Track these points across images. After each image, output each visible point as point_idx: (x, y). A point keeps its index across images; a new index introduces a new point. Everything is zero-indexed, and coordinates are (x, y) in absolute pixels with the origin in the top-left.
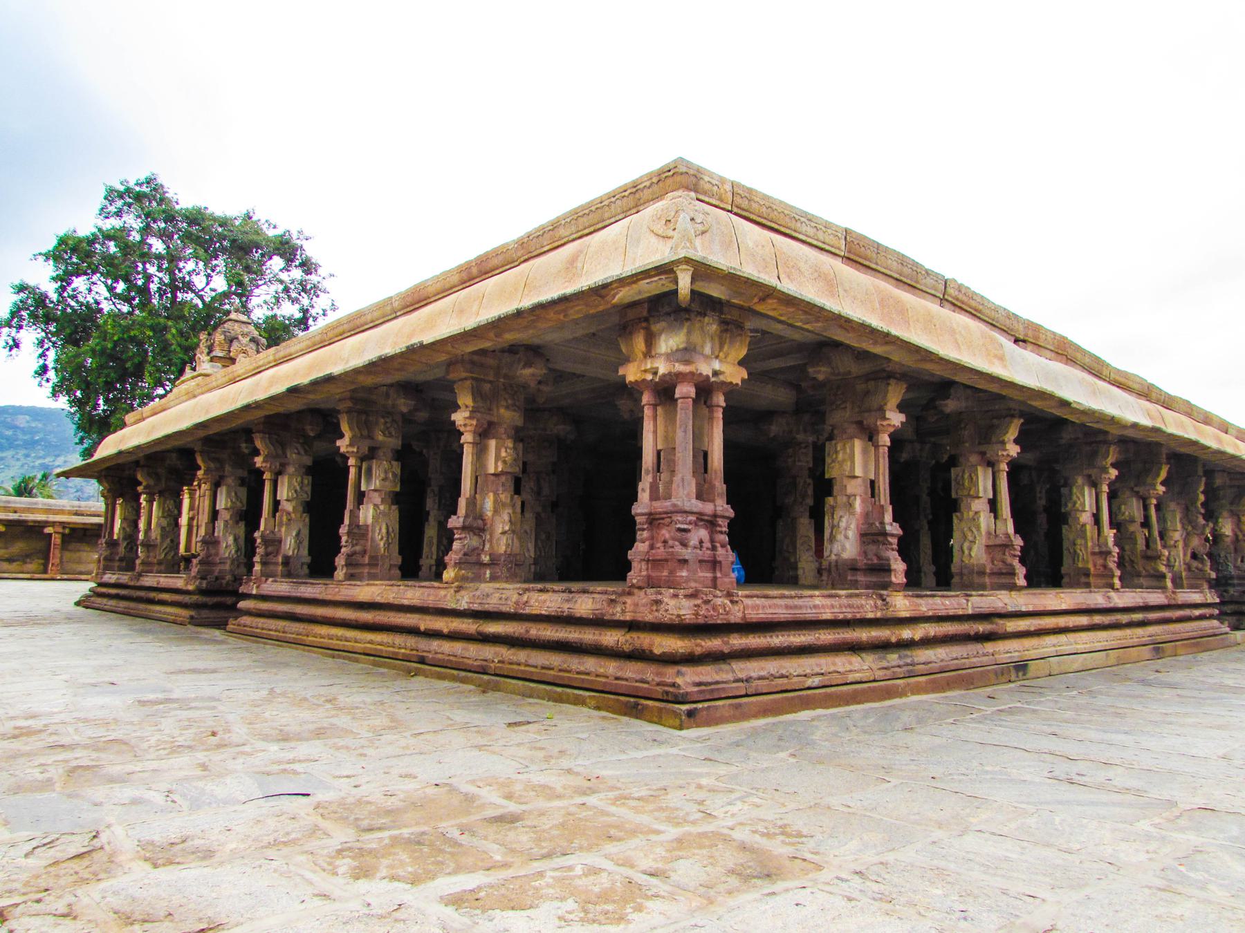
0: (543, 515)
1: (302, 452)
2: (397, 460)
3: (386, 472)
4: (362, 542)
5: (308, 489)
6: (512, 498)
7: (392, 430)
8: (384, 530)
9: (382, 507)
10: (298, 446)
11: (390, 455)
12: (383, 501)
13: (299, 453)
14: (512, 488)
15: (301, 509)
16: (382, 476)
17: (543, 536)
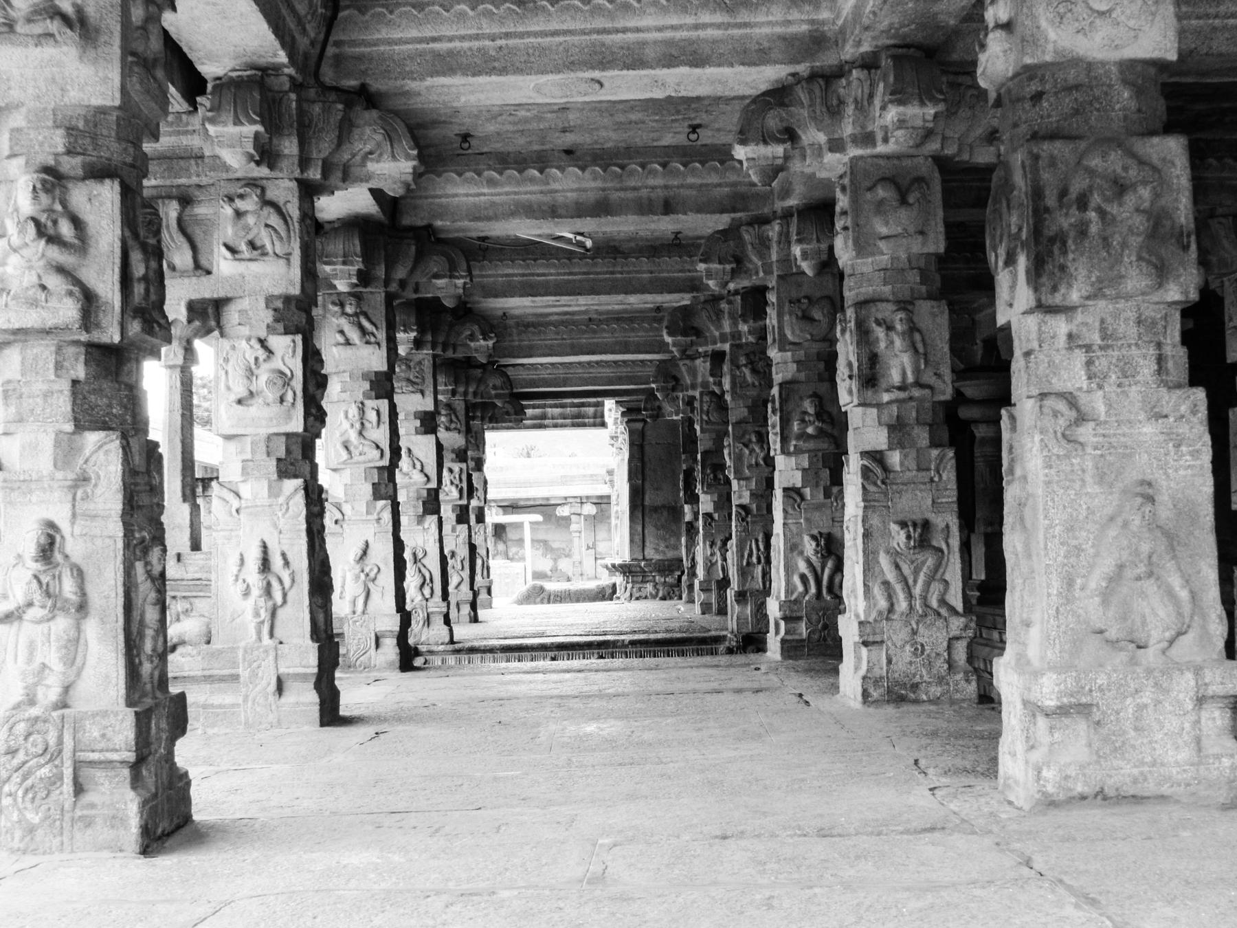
0: (895, 458)
1: (354, 335)
2: (286, 333)
3: (250, 374)
4: (200, 605)
5: (381, 435)
6: (66, 451)
7: (265, 238)
8: (253, 563)
9: (245, 490)
10: (344, 323)
11: (267, 316)
12: (245, 471)
13: (348, 343)
14: (63, 403)
15: (368, 489)
16: (240, 390)
17: (899, 537)
